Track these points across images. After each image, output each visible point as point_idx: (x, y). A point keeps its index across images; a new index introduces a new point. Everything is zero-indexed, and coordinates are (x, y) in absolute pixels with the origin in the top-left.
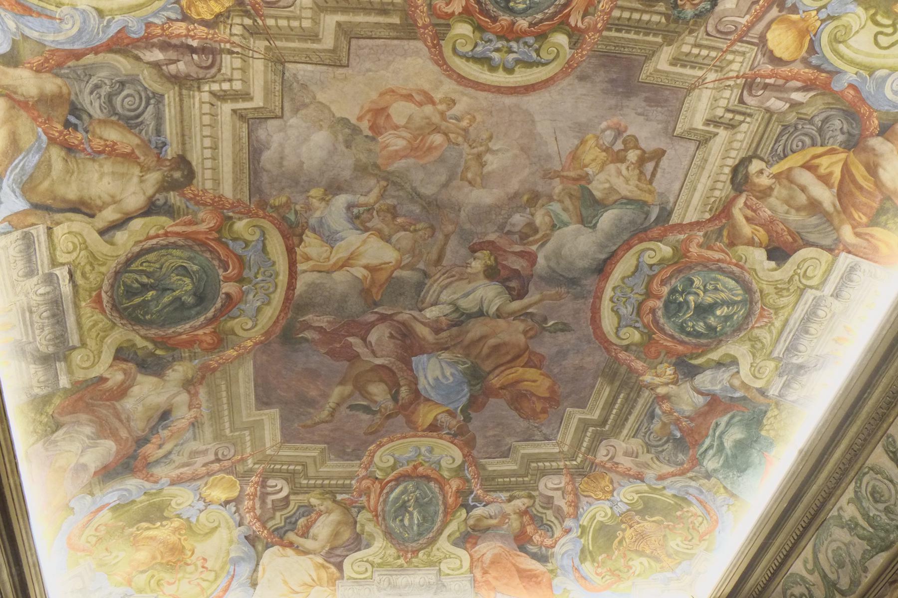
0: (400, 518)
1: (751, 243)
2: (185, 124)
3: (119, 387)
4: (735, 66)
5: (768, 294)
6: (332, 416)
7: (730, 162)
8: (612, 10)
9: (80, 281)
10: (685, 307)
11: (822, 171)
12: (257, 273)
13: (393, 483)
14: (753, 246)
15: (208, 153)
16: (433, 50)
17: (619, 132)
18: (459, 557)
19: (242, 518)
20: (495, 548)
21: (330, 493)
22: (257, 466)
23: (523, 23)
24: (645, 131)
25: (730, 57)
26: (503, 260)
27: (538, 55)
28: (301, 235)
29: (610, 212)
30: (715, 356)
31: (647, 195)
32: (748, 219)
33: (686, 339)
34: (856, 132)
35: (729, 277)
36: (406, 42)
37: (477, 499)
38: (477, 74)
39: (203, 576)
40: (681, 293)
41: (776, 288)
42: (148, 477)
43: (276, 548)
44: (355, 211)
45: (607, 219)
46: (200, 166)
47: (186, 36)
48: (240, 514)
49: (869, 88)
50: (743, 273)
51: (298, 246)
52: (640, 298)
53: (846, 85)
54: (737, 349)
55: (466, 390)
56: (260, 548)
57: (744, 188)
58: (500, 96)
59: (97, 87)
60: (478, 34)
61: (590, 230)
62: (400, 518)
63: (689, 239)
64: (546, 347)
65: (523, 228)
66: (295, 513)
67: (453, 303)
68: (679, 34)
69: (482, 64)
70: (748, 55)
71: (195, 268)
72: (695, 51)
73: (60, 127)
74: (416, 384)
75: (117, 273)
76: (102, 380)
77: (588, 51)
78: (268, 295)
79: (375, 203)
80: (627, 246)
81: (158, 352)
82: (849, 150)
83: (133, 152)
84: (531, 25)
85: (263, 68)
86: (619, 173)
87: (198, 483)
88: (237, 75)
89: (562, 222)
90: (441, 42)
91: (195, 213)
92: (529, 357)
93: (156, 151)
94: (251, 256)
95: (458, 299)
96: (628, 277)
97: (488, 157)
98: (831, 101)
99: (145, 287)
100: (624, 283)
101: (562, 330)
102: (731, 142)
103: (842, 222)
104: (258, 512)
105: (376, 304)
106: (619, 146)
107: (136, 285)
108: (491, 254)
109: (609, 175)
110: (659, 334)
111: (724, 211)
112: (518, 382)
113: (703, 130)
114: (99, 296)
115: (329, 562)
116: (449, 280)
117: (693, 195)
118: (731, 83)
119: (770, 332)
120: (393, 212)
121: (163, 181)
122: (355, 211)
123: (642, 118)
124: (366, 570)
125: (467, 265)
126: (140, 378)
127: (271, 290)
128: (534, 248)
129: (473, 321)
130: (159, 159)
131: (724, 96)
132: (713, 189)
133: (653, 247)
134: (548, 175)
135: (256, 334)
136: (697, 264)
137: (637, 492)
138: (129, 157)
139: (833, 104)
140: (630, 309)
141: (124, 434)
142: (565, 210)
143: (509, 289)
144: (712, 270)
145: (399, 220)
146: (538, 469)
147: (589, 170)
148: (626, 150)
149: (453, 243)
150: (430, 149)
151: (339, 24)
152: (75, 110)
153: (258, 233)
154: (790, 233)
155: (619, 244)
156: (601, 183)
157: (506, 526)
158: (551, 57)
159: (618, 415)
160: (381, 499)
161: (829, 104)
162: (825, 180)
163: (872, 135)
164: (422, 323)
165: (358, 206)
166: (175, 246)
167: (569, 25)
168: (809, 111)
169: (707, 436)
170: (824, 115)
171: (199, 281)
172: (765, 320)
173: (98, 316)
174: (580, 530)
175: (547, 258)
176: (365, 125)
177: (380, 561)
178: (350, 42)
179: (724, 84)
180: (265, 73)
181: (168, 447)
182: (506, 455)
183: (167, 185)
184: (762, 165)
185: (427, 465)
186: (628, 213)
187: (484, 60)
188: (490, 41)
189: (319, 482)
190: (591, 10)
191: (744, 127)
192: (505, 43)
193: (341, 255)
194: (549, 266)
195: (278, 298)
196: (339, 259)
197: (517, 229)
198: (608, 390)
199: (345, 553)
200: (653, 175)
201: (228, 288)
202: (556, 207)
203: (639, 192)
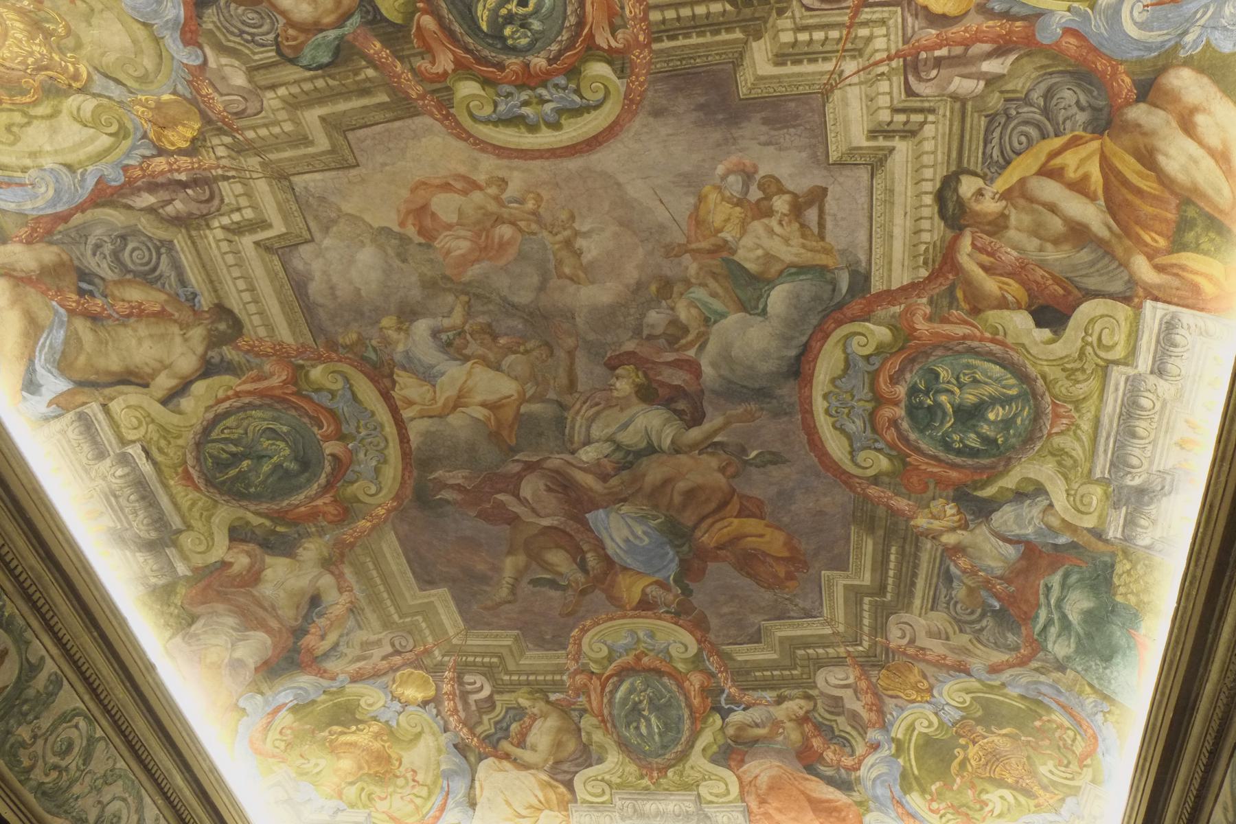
0: (635, 724)
1: (1003, 304)
2: (208, 268)
3: (249, 571)
4: (880, 43)
5: (1056, 381)
6: (514, 594)
7: (927, 186)
9: (159, 458)
10: (940, 413)
11: (1071, 174)
12: (358, 427)
13: (615, 679)
14: (1007, 308)
15: (247, 297)
16: (447, 123)
17: (748, 176)
18: (722, 779)
19: (446, 723)
20: (771, 767)
22: (446, 659)
23: (539, 62)
24: (786, 165)
25: (864, 32)
27: (582, 97)
28: (391, 375)
29: (778, 288)
30: (1010, 481)
31: (824, 256)
33: (958, 460)
34: (1102, 103)
35: (989, 361)
36: (409, 121)
37: (731, 699)
38: (516, 140)
39: (415, 791)
40: (927, 393)
43: (490, 760)
44: (444, 337)
45: (778, 298)
46: (244, 312)
49: (1097, 27)
52: (869, 406)
55: (671, 553)
56: (472, 759)
58: (558, 161)
60: (490, 91)
61: (760, 319)
62: (635, 724)
63: (909, 312)
64: (759, 486)
66: (504, 718)
67: (610, 439)
69: (517, 126)
70: (891, 22)
71: (285, 429)
72: (803, 37)
74: (604, 549)
75: (198, 445)
76: (224, 565)
78: (381, 451)
79: (464, 323)
80: (821, 334)
81: (279, 529)
82: (1102, 134)
84: (550, 61)
85: (268, 188)
86: (771, 232)
88: (243, 202)
89: (715, 312)
90: (452, 111)
91: (260, 367)
92: (741, 504)
93: (188, 304)
94: (342, 406)
96: (840, 377)
97: (580, 243)
98: (1045, 62)
99: (236, 458)
100: (836, 387)
101: (774, 463)
103: (1128, 252)
104: (462, 715)
105: (513, 450)
106: (755, 194)
107: (225, 456)
108: (637, 369)
110: (915, 456)
111: (945, 262)
114: (186, 471)
115: (557, 780)
116: (596, 408)
117: (891, 246)
118: (883, 69)
119: (1079, 439)
122: (444, 337)
123: (771, 149)
124: (604, 792)
125: (611, 388)
126: (269, 560)
127: (382, 445)
128: (691, 353)
129: (645, 461)
130: (196, 313)
131: (881, 90)
132: (917, 232)
133: (860, 330)
134: (673, 252)
136: (935, 347)
139: (1049, 66)
140: (859, 423)
141: (274, 624)
142: (714, 295)
143: (679, 413)
144: (959, 353)
145: (502, 341)
148: (768, 198)
149: (582, 363)
150: (503, 246)
151: (323, 119)
153: (340, 378)
154: (1057, 281)
155: (810, 332)
156: (751, 250)
157: (781, 738)
158: (600, 95)
159: (898, 577)
160: (605, 700)
161: (1042, 67)
162: (1080, 187)
163: (1128, 104)
164: (580, 468)
166: (251, 406)
167: (599, 48)
168: (1018, 85)
170: (1043, 87)
172: (1065, 421)
173: (194, 495)
175: (714, 365)
176: (411, 231)
177: (619, 781)
178: (346, 137)
179: (873, 74)
180: (273, 193)
181: (332, 638)
182: (756, 638)
184: (980, 183)
185: (652, 654)
186: (806, 286)
188: (509, 95)
189: (523, 678)
190: (617, 21)
191: (929, 130)
192: (529, 92)
193: (447, 394)
194: (720, 376)
195: (394, 452)
196: (447, 399)
198: (870, 542)
199: (573, 769)
200: (821, 225)
201: (331, 447)
203: (810, 254)
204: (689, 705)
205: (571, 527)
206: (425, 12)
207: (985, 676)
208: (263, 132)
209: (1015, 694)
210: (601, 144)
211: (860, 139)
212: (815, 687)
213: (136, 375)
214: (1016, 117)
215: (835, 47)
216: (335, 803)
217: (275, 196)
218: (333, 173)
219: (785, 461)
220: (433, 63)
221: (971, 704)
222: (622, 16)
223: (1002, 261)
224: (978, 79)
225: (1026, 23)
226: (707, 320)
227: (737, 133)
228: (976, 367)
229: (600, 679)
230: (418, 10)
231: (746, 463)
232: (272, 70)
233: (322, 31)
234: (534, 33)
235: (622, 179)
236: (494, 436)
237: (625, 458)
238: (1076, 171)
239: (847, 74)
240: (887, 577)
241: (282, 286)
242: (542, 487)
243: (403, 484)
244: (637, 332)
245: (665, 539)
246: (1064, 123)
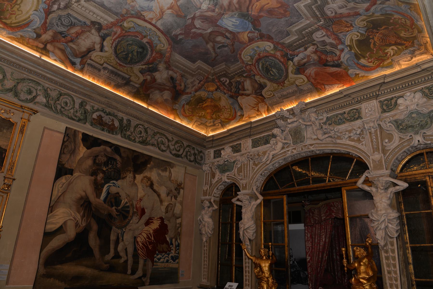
9: (112, 64)
12: (146, 32)
18: (301, 78)
19: (224, 92)
20: (313, 69)
21: (240, 75)
28: (141, 15)
37: (291, 55)
42: (187, 93)
43: (240, 97)
59: (57, 25)
73: (64, 39)
74: (229, 31)
75: (117, 56)
76: (145, 80)
78: (156, 35)
81: (150, 66)
87: (203, 88)
94: (140, 29)
99: (127, 55)
104: (226, 89)
105: (185, 17)
114: (119, 64)
124: (271, 94)
126: (154, 74)
130: (89, 27)
137: (363, 20)
138: (83, 32)
152: (61, 33)
153: (132, 23)
173: (125, 68)
174: (348, 48)
181: (183, 85)
185: (262, 52)
193: (158, 11)
195: (159, 33)
201: (145, 41)
204: (281, 62)
205: (216, 29)
207: (366, 13)
209: (379, 15)
212: (314, 40)
213: (89, 49)
216: (212, 120)
221: (367, 24)
236: (178, 16)
241: (99, 8)
243: (168, 40)
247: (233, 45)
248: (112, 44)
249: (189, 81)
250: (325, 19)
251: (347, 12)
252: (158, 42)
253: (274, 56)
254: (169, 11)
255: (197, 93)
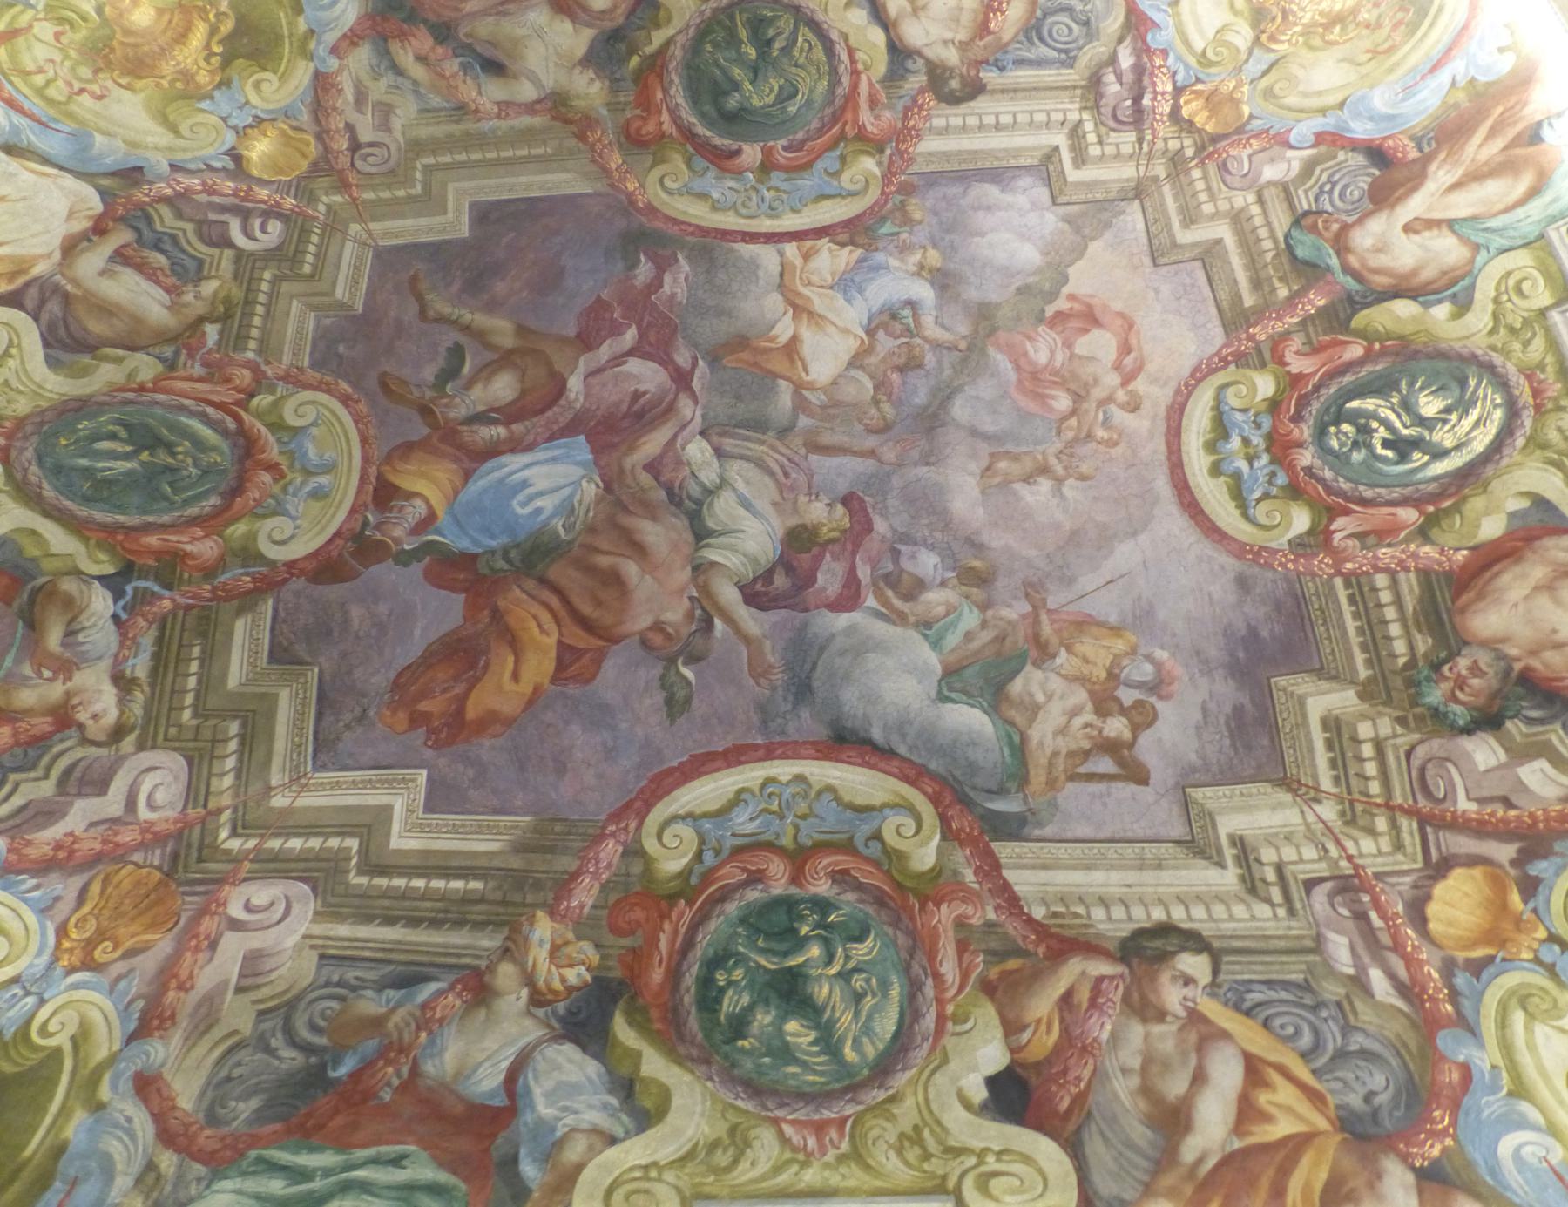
1: (1011, 1028)
4: (1367, 845)
5: (892, 1118)
6: (436, 320)
7: (1178, 914)
8: (1387, 570)
10: (784, 946)
11: (1263, 1098)
12: (777, 190)
15: (989, 120)
22: (322, 208)
23: (1306, 457)
24: (1173, 735)
25: (1381, 824)
26: (832, 553)
27: (1258, 501)
28: (852, 243)
29: (985, 718)
30: (654, 1065)
31: (1043, 779)
32: (1067, 999)
34: (1388, 1124)
35: (902, 1015)
36: (1217, 322)
37: (144, 597)
38: (1194, 427)
41: (916, 1128)
42: (352, 38)
44: (907, 312)
45: (968, 719)
47: (1155, 93)
48: (201, 171)
49: (1488, 1105)
50: (924, 1039)
51: (831, 241)
52: (786, 841)
53: (1461, 1058)
54: (693, 1106)
55: (494, 543)
57: (1135, 961)
58: (1166, 469)
60: (1264, 406)
61: (933, 694)
62: (123, 434)
63: (969, 896)
64: (622, 677)
65: (910, 574)
66: (184, 251)
67: (723, 483)
68: (1389, 702)
69: (1213, 430)
70: (1400, 857)
71: (792, 109)
72: (1367, 750)
74: (512, 451)
77: (1296, 569)
78: (734, 207)
80: (914, 774)
81: (635, 61)
82: (1343, 1129)
83: (990, 33)
84: (1308, 470)
86: (1075, 712)
87: (305, 117)
88: (1110, 150)
90: (1232, 367)
91: (891, 107)
93: (991, 60)
94: (807, 183)
95: (734, 489)
96: (838, 799)
97: (1045, 485)
98: (1413, 1045)
99: (764, 45)
100: (819, 793)
101: (670, 701)
102: (1219, 898)
104: (203, 198)
105: (714, 359)
106: (1127, 696)
109: (1062, 698)
110: (688, 915)
111: (1062, 942)
112: (514, 643)
113: (1217, 838)
117: (1074, 868)
118: (1334, 852)
119: (777, 1169)
120: (911, 365)
121: (945, 68)
123: (1198, 716)
125: (813, 493)
126: (588, 34)
128: (871, 601)
129: (681, 523)
130: (980, 63)
132: (1104, 902)
133: (926, 826)
134: (1033, 590)
135: (653, 193)
136: (912, 934)
138: (983, 29)
140: (750, 828)
142: (969, 636)
145: (895, 377)
146: (217, 740)
147: (1062, 657)
148: (1124, 711)
150: (1042, 398)
153: (858, 187)
154: (1080, 1099)
156: (1043, 686)
158: (1263, 520)
159: (405, 895)
160: (187, 402)
161: (1405, 1045)
162: (1247, 1112)
163: (1405, 1158)
164: (675, 437)
165: (915, 315)
167: (1331, 520)
168: (1365, 1015)
169: (342, 1146)
170: (1375, 1046)
171: (767, 115)
172: (811, 1142)
175: (851, 630)
176: (1062, 304)
179: (1324, 839)
180: (1118, 180)
181: (418, 72)
182: (282, 655)
183: (937, 75)
184: (1204, 977)
187: (1221, 428)
188: (1258, 426)
190: (1371, 540)
191: (1263, 910)
192: (1262, 446)
194: (833, 636)
196: (809, 299)
197: (906, 564)
200: (1091, 777)
201: (751, 154)
202: (970, 619)
203: (1043, 761)
204: (147, 528)
205: (560, 414)
206: (1369, 350)
208: (1200, 185)
210: (1192, 517)
211: (1228, 825)
212: (141, 747)
214: (1318, 1017)
215: (1355, 789)
217: (1114, 181)
218: (1145, 241)
219: (672, 717)
220: (1297, 353)
222: (1378, 545)
223: (1086, 1020)
224: (1355, 966)
225: (1455, 1016)
226: (928, 625)
227: (1219, 674)
228: (885, 995)
229: (238, 403)
230: (1371, 343)
231: (671, 661)
232: (1285, 205)
233: (1338, 253)
234: (1347, 456)
235: (1143, 538)
236: (741, 342)
237: (689, 497)
238: (1270, 1103)
239: (1317, 808)
240: (410, 876)
241: (997, 158)
242: (642, 388)
243: (675, 221)
244: (906, 538)
245: (522, 536)
246: (1337, 1079)
247: (426, 411)
248: (851, 52)
249: (406, 112)
250: (235, 859)
251: (206, 980)
252: (698, 185)
253: (212, 522)
254: (784, 330)
255: (302, 74)
